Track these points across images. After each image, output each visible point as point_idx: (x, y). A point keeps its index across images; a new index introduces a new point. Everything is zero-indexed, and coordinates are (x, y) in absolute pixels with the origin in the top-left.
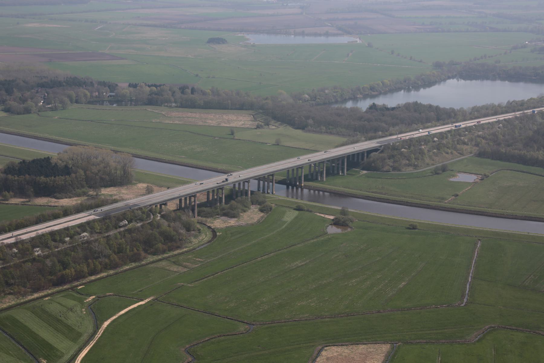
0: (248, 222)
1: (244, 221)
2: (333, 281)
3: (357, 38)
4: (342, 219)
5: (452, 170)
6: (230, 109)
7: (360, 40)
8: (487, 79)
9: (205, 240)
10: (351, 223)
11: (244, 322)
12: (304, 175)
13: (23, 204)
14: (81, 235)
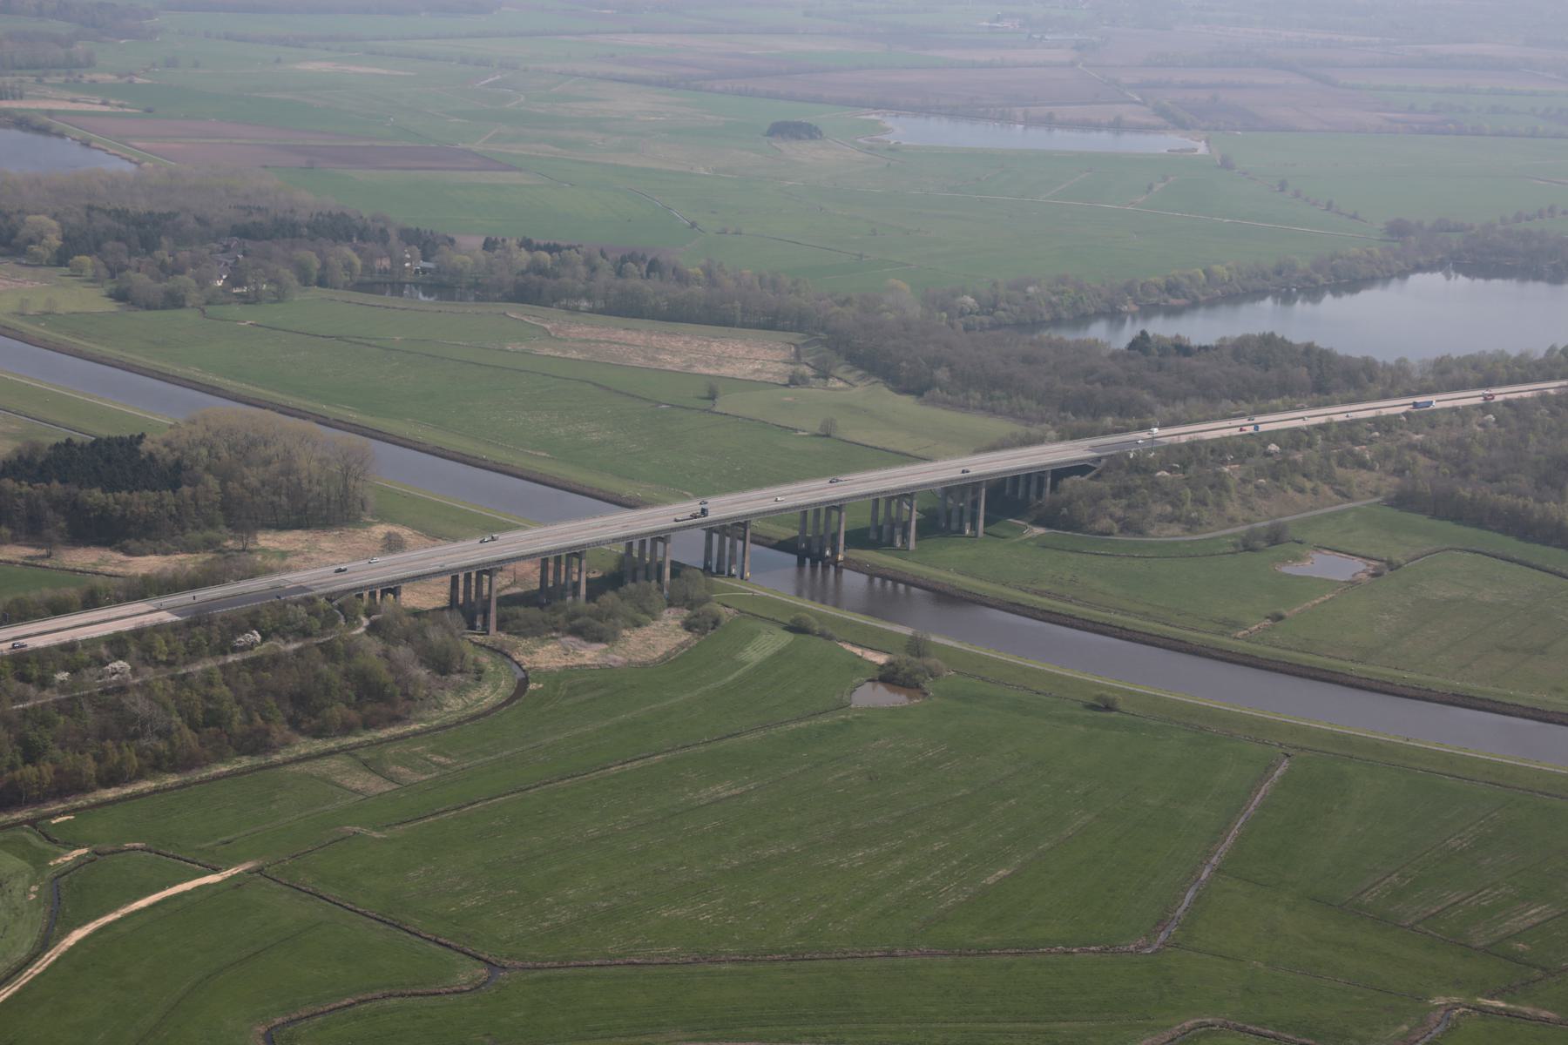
0: (633, 658)
1: (624, 653)
2: (799, 850)
3: (1200, 141)
4: (908, 665)
5: (1300, 542)
7: (1208, 146)
8: (1538, 277)
9: (486, 703)
10: (931, 679)
11: (479, 959)
12: (846, 532)
13: (28, 563)
14: (107, 667)
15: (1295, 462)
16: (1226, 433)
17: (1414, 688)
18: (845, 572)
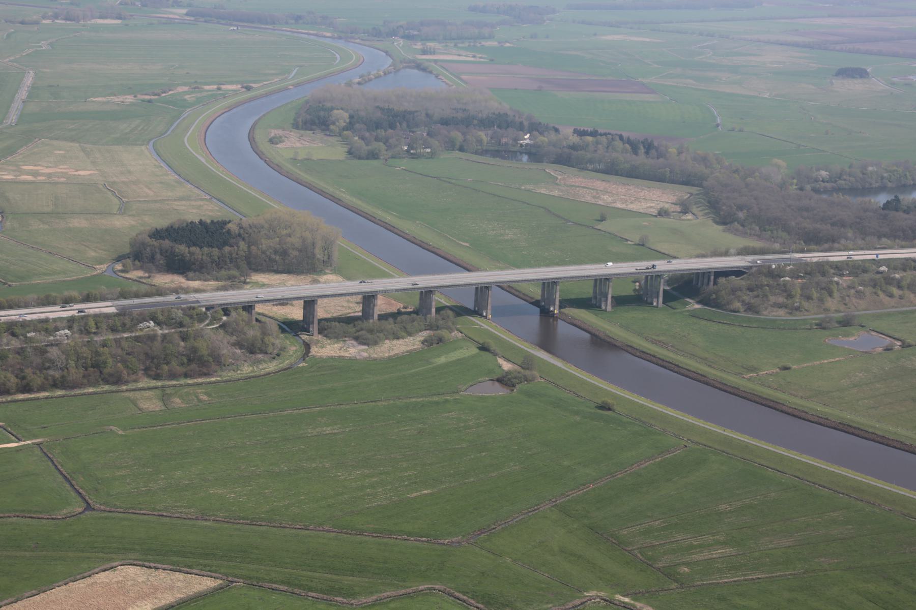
5: (863, 327)
6: (668, 183)
10: (526, 382)
14: (57, 333)
15: (893, 279)
18: (559, 320)
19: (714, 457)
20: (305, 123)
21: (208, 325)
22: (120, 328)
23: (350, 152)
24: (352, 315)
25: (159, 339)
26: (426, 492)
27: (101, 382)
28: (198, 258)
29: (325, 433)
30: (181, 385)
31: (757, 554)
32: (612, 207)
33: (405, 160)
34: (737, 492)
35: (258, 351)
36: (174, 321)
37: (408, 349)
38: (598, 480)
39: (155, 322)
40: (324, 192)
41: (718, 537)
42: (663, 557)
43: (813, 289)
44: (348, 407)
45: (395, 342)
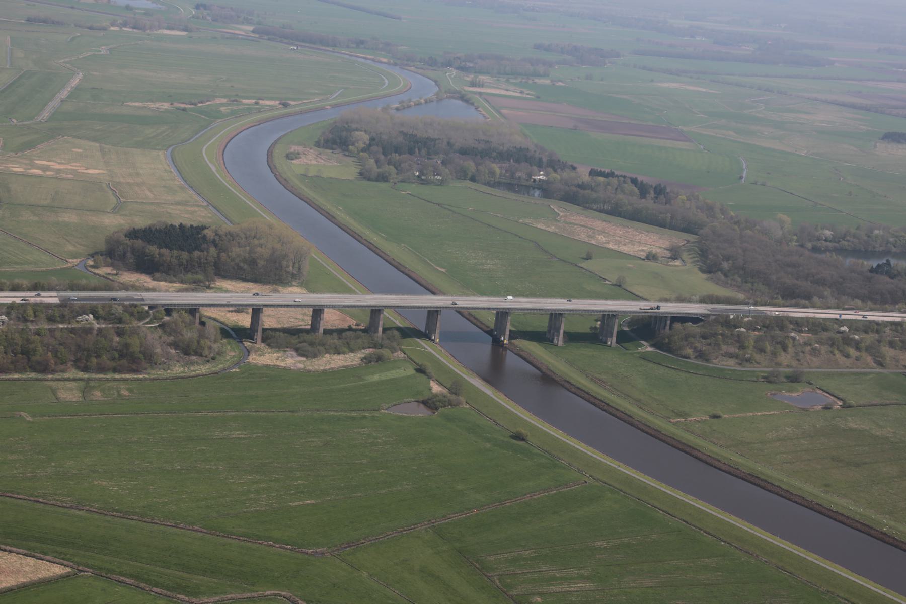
10: (450, 407)
16: (811, 315)
17: (729, 466)
18: (508, 351)
19: (610, 495)
20: (326, 141)
21: (147, 323)
22: (58, 319)
23: (361, 174)
24: (303, 327)
25: (95, 332)
26: (309, 502)
27: (28, 369)
28: (166, 260)
29: (231, 437)
30: (107, 379)
31: (616, 591)
32: (605, 248)
33: (414, 185)
34: (620, 531)
35: (192, 353)
36: (113, 316)
37: (346, 364)
38: (485, 506)
39: (94, 316)
40: (321, 209)
41: (583, 571)
42: (521, 586)
43: (767, 342)
44: (264, 414)
45: (336, 357)
